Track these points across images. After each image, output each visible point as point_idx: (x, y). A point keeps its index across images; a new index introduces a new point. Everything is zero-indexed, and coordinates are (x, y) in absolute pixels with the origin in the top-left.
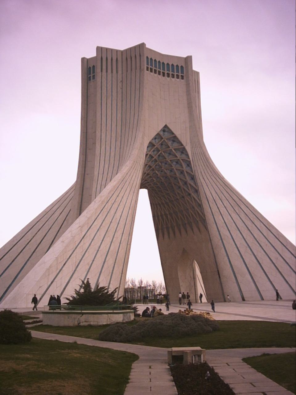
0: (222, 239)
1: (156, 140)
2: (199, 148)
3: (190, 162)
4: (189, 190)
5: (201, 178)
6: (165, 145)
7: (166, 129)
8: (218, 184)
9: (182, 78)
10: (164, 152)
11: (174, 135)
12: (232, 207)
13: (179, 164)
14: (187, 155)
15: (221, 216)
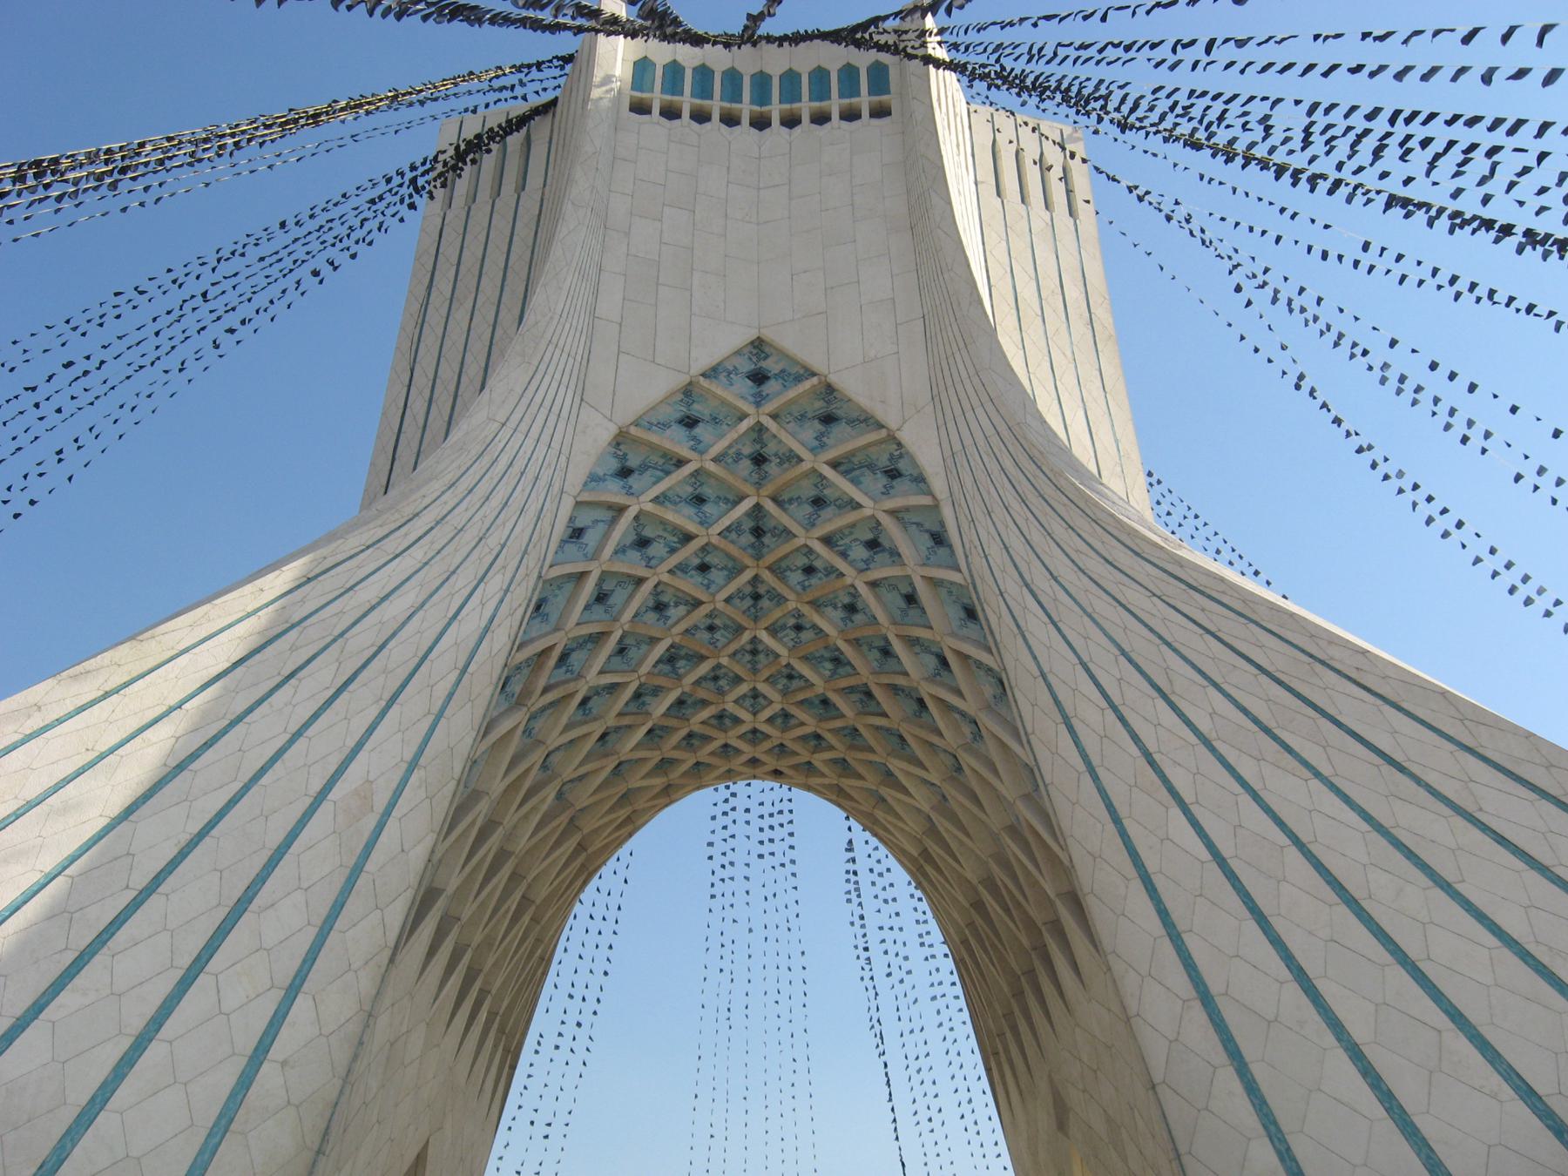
0: (1206, 999)
1: (698, 430)
2: (979, 411)
3: (936, 507)
4: (959, 693)
5: (1012, 586)
6: (776, 455)
7: (760, 366)
8: (1134, 597)
9: (880, 112)
10: (774, 499)
11: (815, 380)
12: (1267, 731)
13: (884, 550)
14: (920, 479)
15: (1176, 812)
